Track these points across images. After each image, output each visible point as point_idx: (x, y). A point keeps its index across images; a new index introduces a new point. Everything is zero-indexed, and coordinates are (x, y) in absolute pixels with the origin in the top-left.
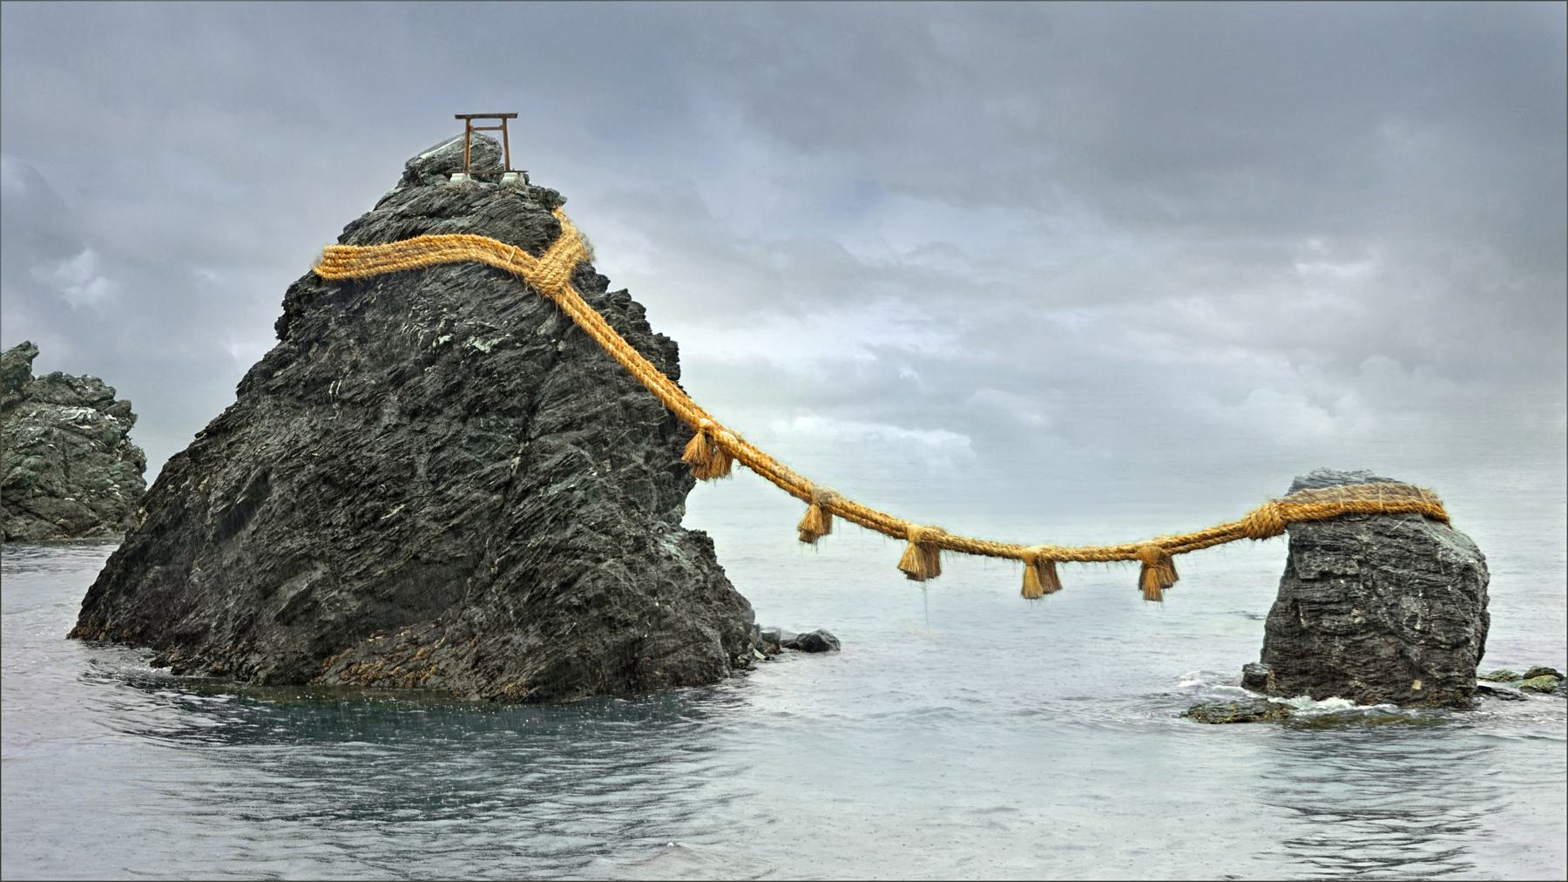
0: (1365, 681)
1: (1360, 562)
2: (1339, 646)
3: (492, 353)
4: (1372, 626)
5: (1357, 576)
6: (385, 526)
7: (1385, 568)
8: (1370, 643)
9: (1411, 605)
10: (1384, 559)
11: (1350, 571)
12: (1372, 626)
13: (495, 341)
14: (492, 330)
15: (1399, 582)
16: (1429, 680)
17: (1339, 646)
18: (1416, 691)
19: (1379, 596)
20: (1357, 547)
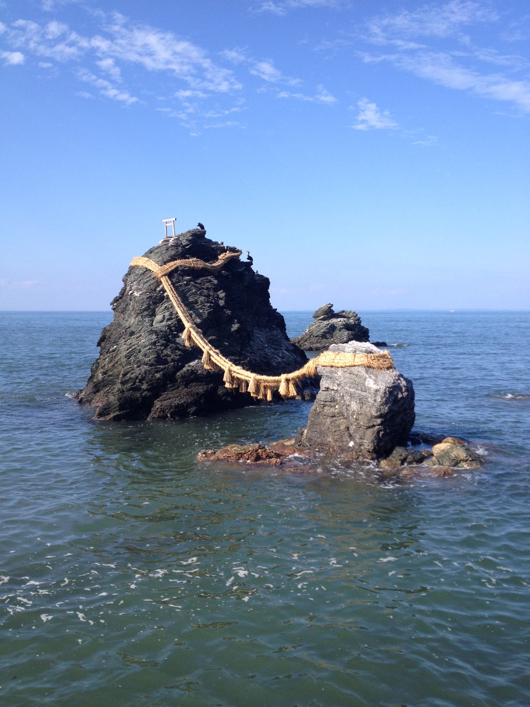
0: (333, 439)
1: (338, 385)
2: (329, 420)
3: (140, 296)
4: (341, 414)
5: (337, 390)
6: (110, 353)
7: (345, 388)
8: (338, 422)
9: (354, 406)
10: (346, 383)
11: (335, 388)
12: (341, 414)
13: (140, 293)
14: (140, 289)
15: (351, 395)
16: (355, 442)
17: (329, 420)
18: (350, 447)
19: (344, 401)
20: (337, 378)
